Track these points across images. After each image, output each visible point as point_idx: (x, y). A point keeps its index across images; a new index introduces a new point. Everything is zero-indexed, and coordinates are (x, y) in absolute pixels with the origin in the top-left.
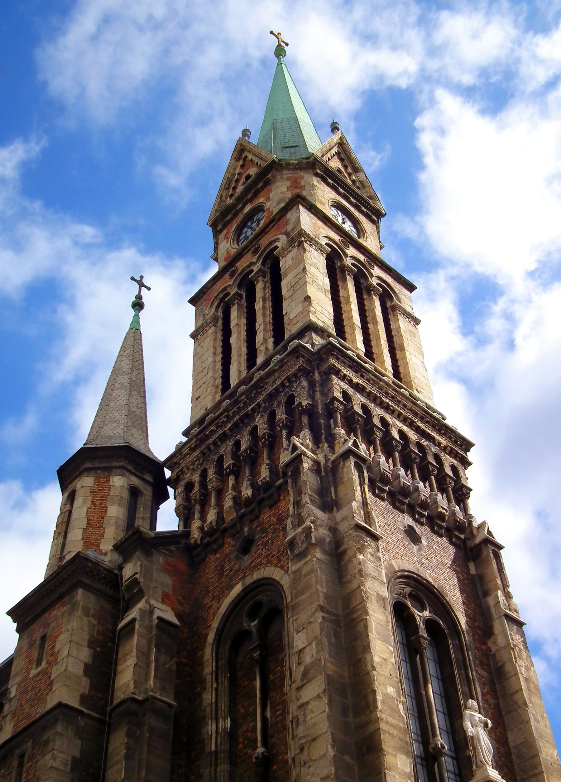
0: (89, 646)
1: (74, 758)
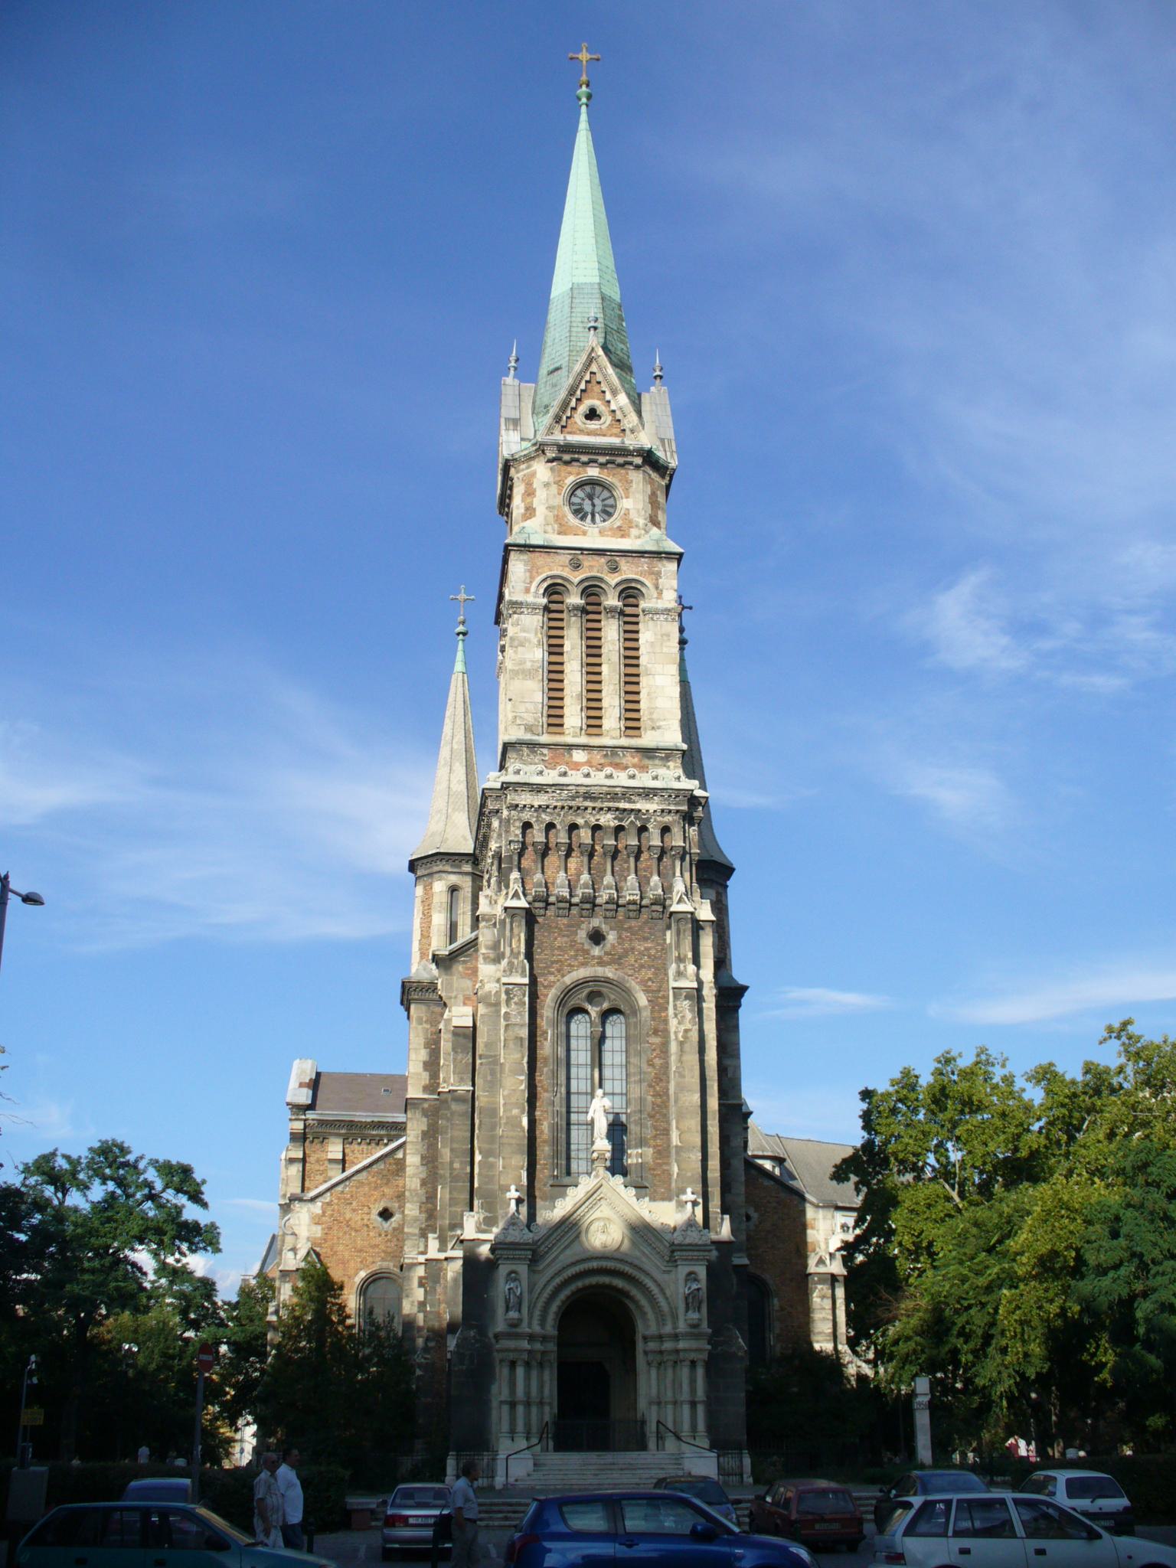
0: (425, 1048)
1: (423, 1131)
